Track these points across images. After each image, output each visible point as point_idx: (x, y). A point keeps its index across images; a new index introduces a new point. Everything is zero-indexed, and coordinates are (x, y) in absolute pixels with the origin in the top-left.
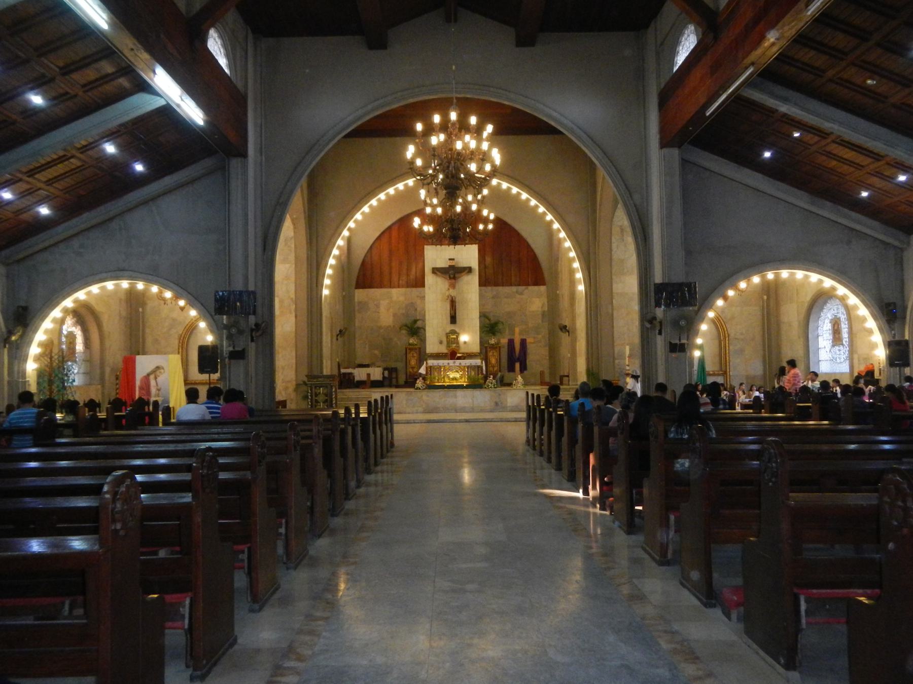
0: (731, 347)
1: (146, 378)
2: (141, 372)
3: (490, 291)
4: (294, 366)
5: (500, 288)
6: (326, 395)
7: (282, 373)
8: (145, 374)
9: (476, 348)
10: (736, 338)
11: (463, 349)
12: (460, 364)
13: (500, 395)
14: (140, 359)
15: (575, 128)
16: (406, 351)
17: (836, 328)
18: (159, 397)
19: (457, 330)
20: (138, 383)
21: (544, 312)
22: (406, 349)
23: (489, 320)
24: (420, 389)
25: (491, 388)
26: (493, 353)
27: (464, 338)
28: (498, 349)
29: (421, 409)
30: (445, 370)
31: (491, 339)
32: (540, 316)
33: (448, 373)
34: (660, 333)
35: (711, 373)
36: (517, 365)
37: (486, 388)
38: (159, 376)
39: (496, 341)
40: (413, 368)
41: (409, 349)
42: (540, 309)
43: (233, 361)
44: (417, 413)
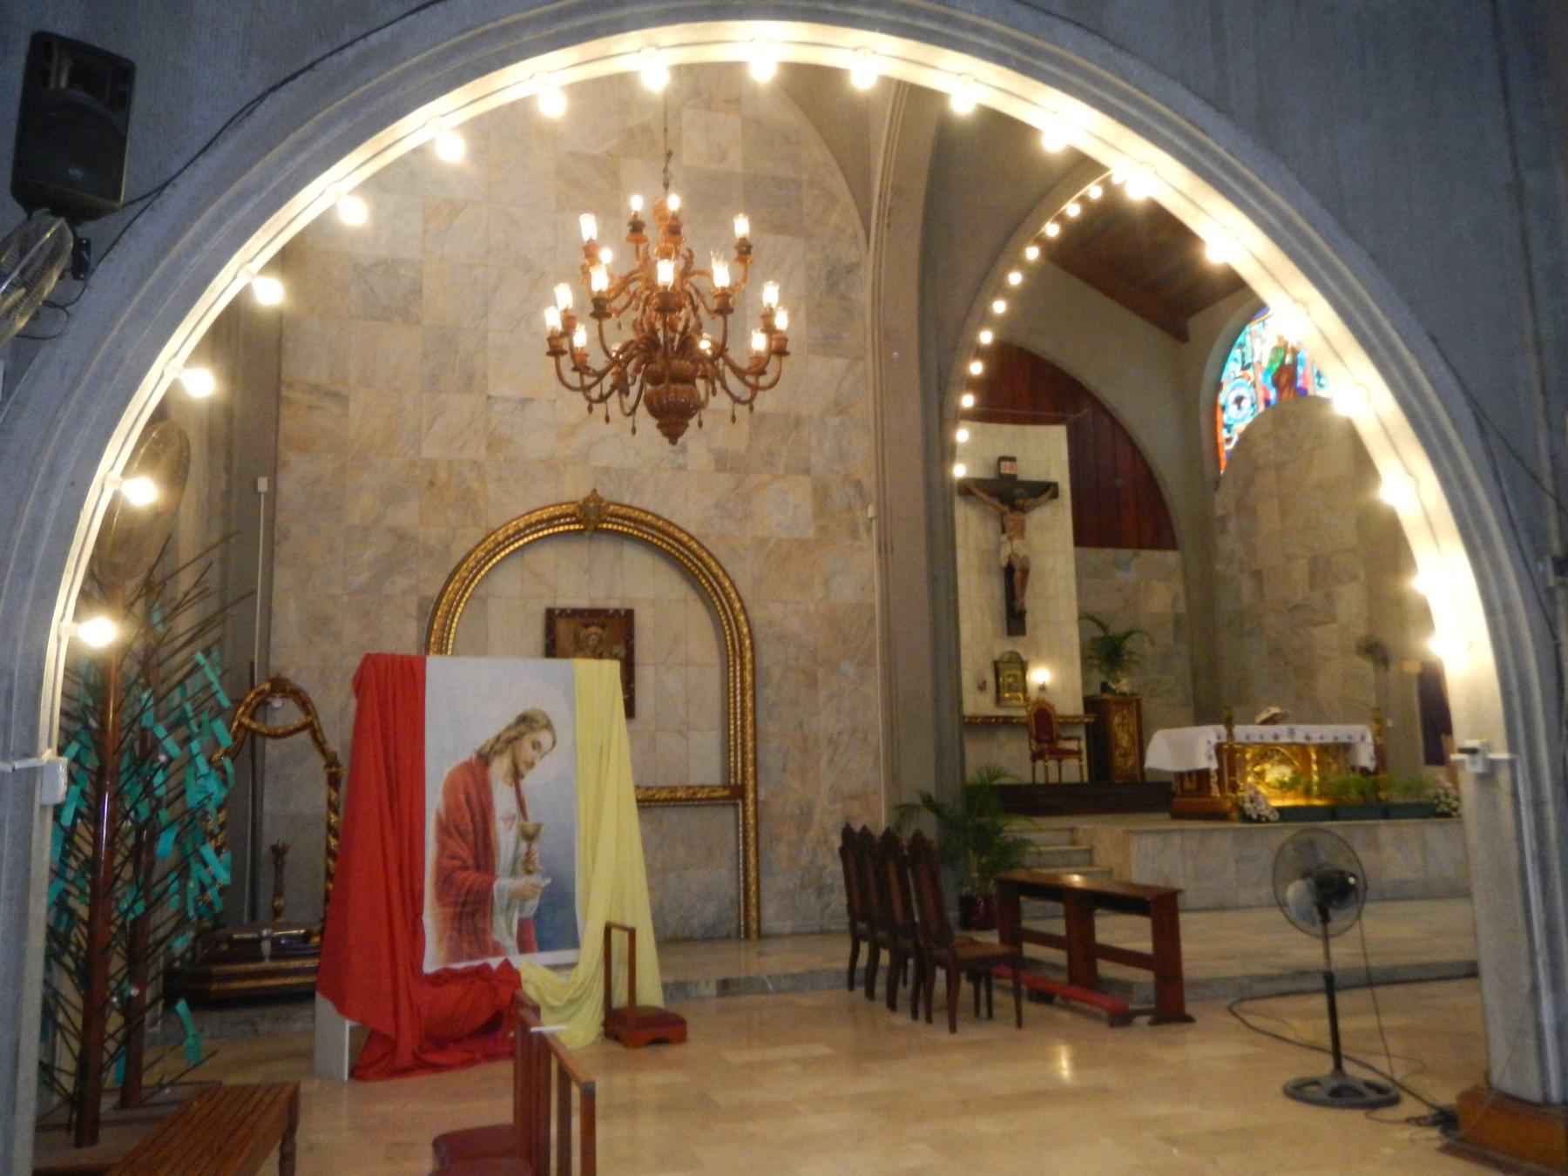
4: (877, 738)
7: (831, 760)
8: (468, 755)
12: (1308, 738)
19: (1025, 658)
20: (434, 801)
21: (1177, 620)
24: (1268, 820)
27: (1040, 675)
28: (1134, 705)
31: (1118, 681)
32: (1170, 626)
38: (531, 765)
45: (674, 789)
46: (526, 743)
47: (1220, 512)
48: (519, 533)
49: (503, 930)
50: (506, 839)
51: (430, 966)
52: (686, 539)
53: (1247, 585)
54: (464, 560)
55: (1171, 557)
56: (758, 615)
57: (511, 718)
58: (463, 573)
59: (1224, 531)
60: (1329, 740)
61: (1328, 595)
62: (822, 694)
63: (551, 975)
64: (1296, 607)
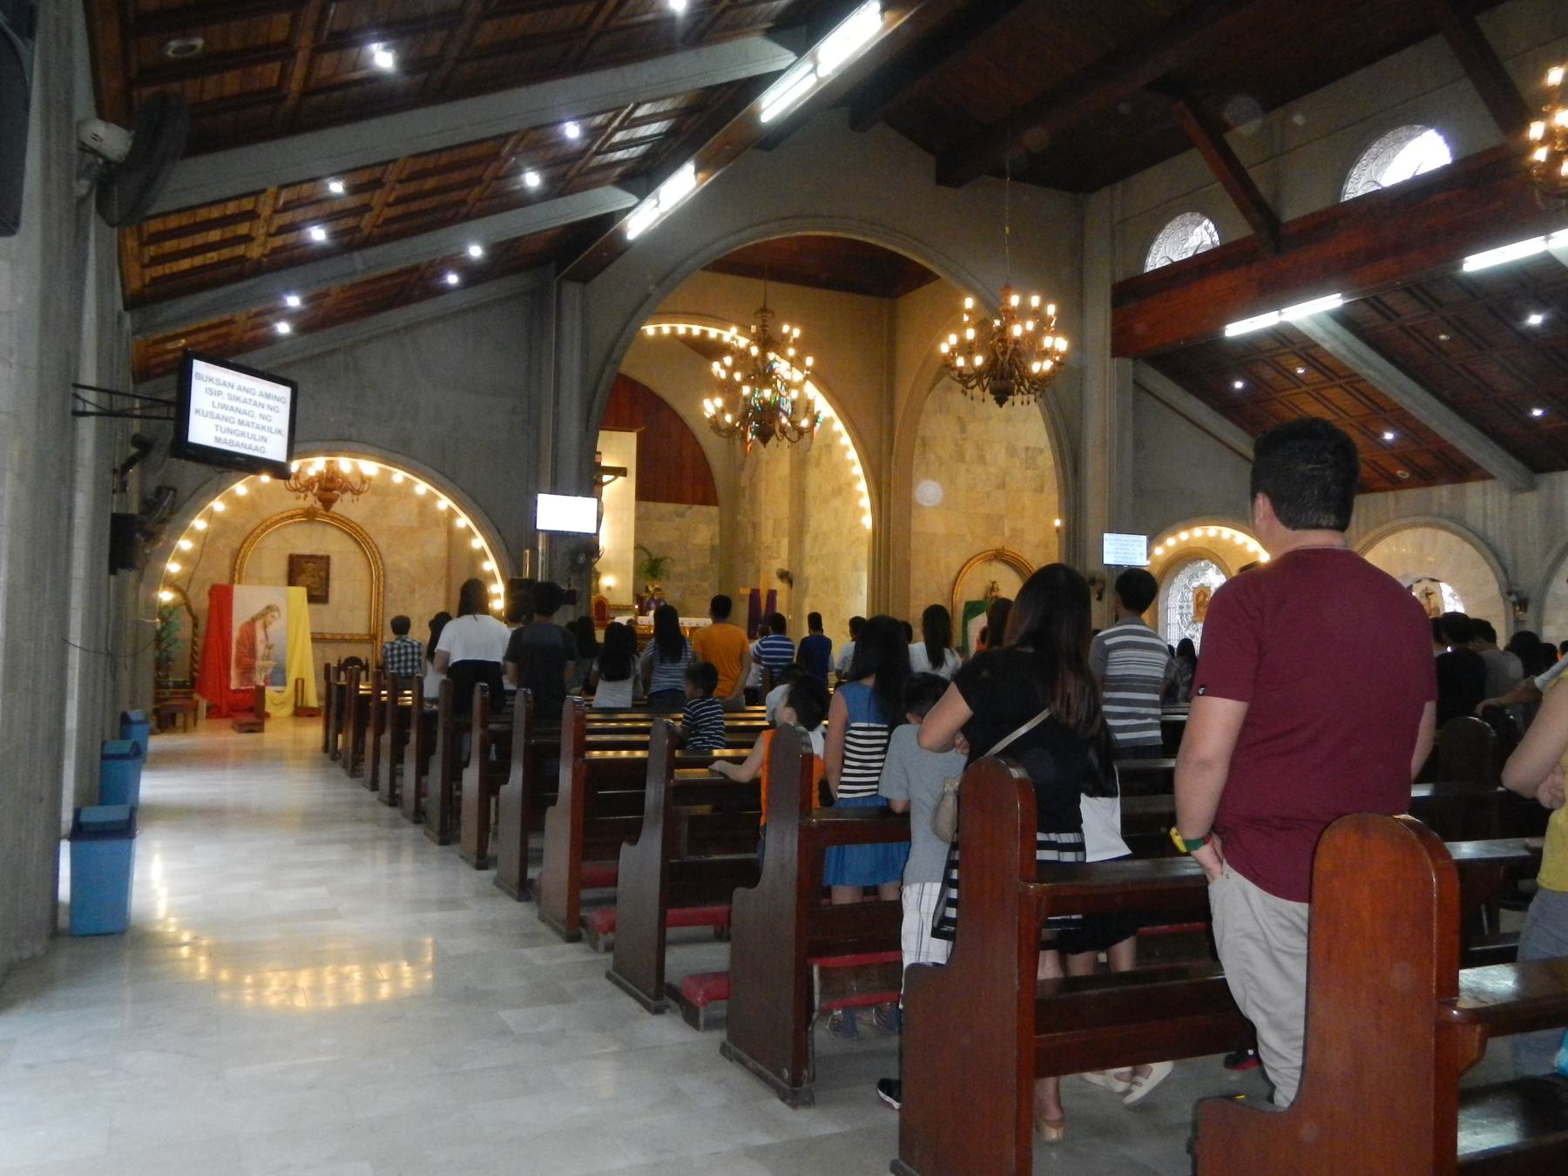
1: (251, 624)
2: (239, 617)
5: (651, 504)
8: (247, 619)
9: (627, 598)
14: (238, 590)
17: (1201, 598)
18: (269, 660)
20: (235, 634)
21: (713, 549)
23: (649, 554)
32: (708, 553)
34: (1100, 598)
38: (270, 623)
42: (709, 541)
45: (343, 635)
46: (269, 615)
47: (743, 485)
48: (277, 522)
50: (261, 648)
52: (355, 526)
53: (750, 531)
54: (252, 533)
55: (714, 510)
56: (388, 561)
57: (264, 606)
58: (251, 539)
59: (744, 496)
60: (694, 625)
61: (778, 542)
62: (417, 596)
63: (276, 694)
64: (767, 547)
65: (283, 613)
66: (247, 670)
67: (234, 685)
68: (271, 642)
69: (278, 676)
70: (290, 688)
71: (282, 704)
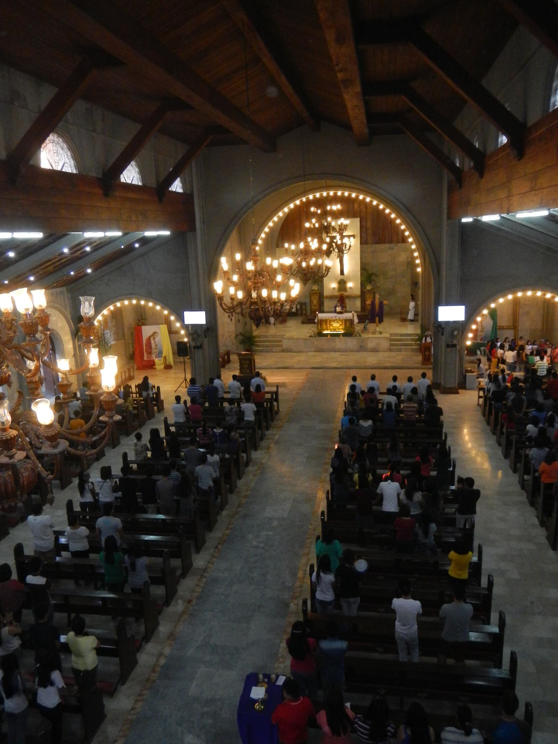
0: (521, 310)
1: (149, 340)
3: (370, 248)
6: (248, 364)
8: (148, 337)
9: (358, 292)
10: (525, 304)
11: (348, 293)
13: (363, 341)
14: (143, 328)
15: (396, 201)
16: (310, 295)
20: (144, 342)
22: (310, 293)
24: (312, 337)
25: (358, 336)
26: (369, 296)
27: (350, 285)
29: (313, 350)
30: (330, 321)
33: (332, 323)
34: (442, 334)
35: (505, 327)
36: (377, 319)
37: (354, 336)
39: (371, 288)
40: (315, 306)
41: (313, 293)
43: (195, 350)
44: (310, 352)
46: (155, 335)
49: (154, 356)
50: (153, 346)
51: (145, 359)
63: (158, 361)
65: (159, 333)
66: (150, 353)
67: (145, 359)
68: (156, 343)
69: (160, 354)
70: (162, 359)
71: (161, 364)
